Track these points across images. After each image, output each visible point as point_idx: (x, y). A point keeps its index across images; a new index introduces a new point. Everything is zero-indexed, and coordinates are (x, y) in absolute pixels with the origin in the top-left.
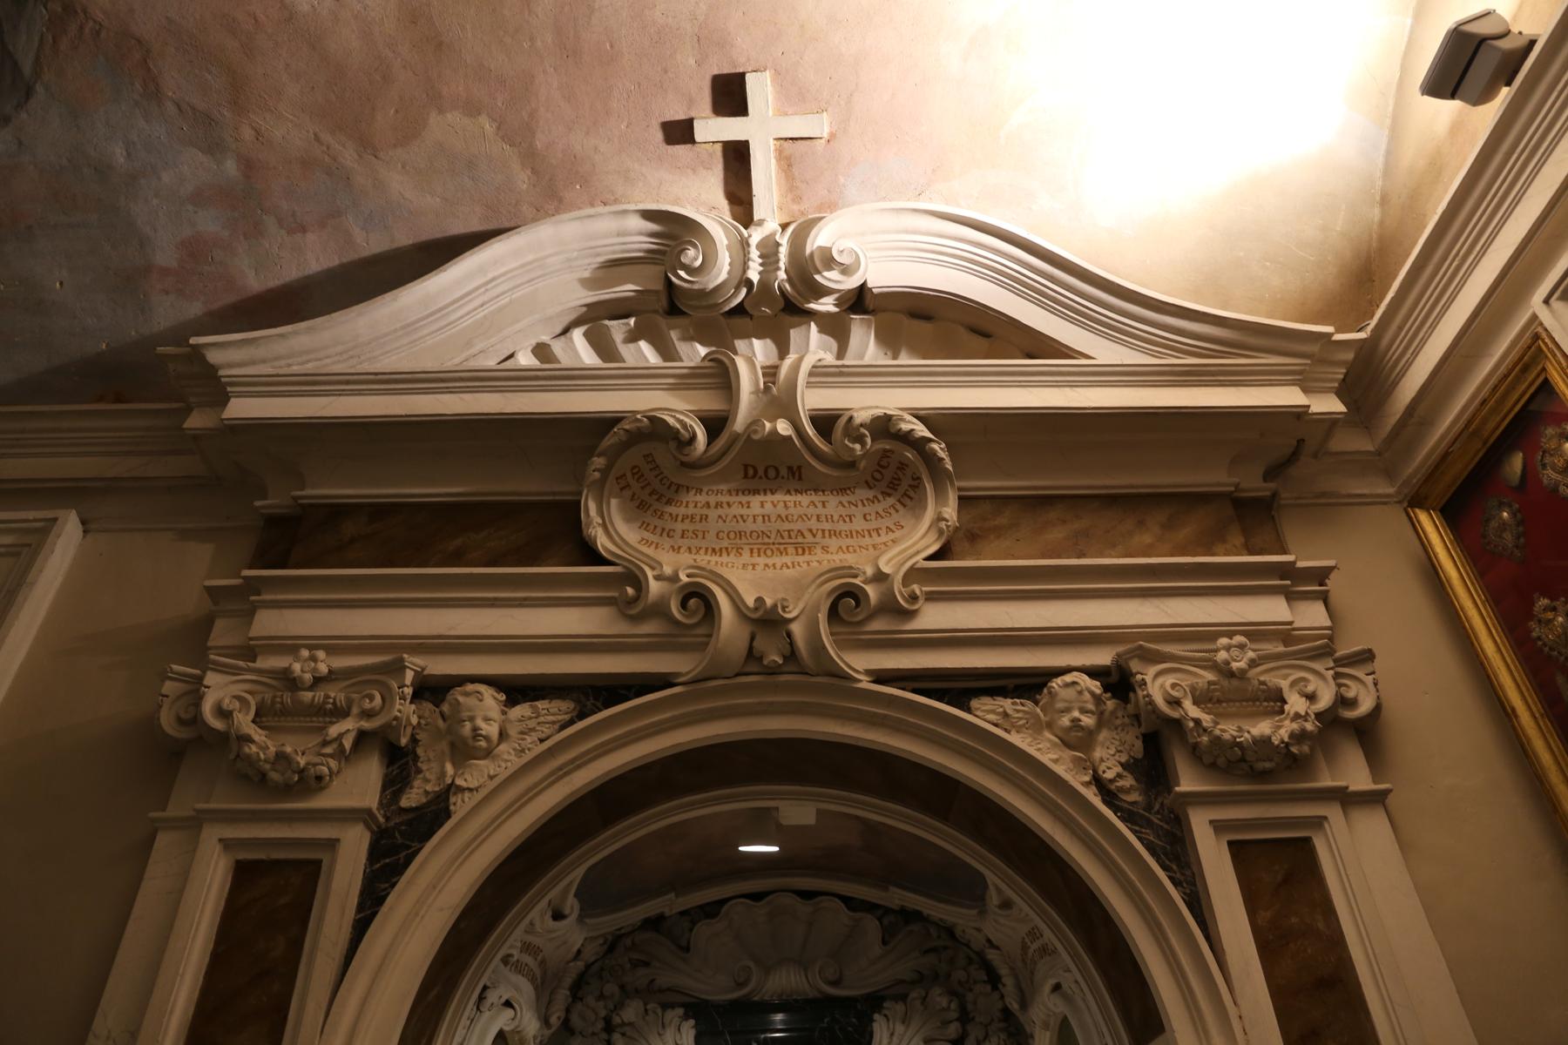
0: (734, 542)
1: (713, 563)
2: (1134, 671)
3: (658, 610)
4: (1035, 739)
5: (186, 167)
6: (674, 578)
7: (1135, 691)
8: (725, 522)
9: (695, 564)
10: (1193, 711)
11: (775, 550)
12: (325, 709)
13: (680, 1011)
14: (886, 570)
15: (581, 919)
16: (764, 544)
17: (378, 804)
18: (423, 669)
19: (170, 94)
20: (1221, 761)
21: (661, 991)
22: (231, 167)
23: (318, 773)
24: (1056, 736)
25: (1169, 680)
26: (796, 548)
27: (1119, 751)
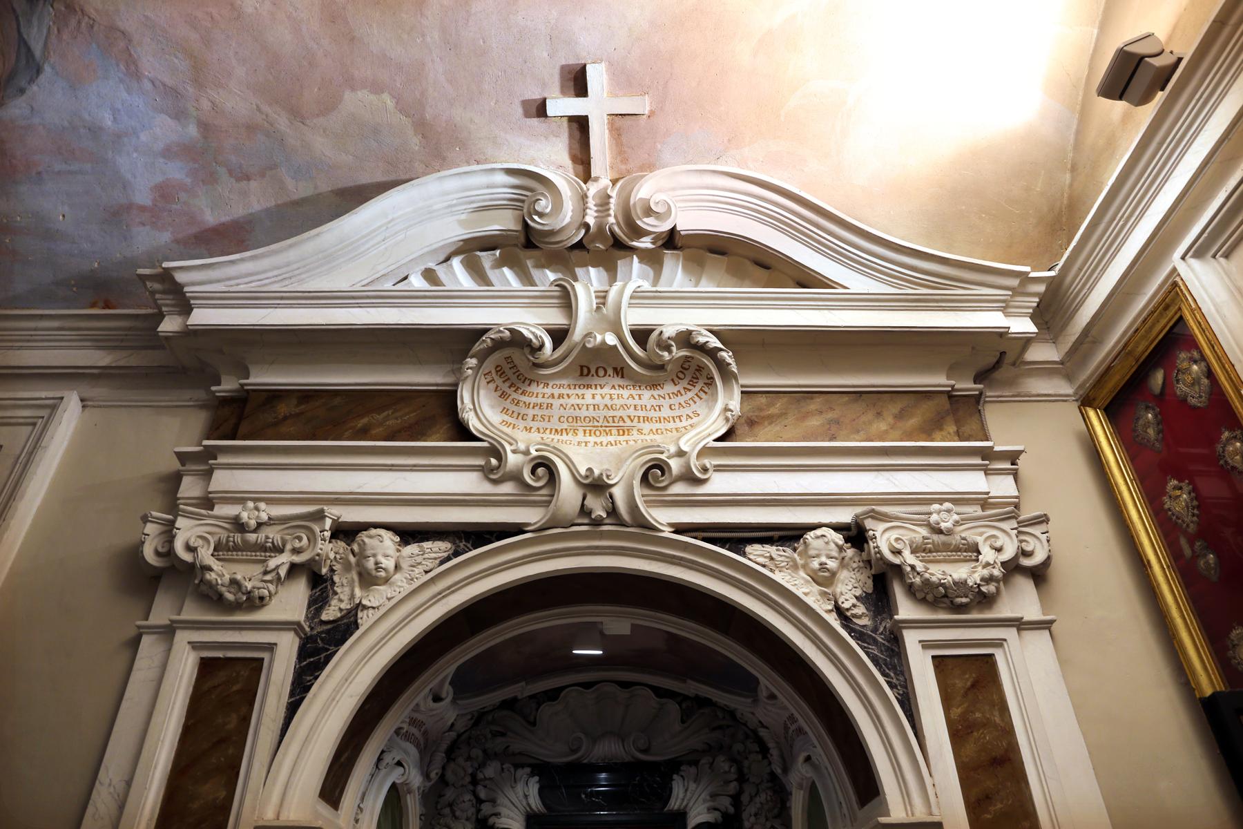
0: (572, 424)
1: (555, 440)
2: (868, 528)
3: (516, 477)
4: (793, 577)
5: (158, 129)
6: (527, 453)
7: (868, 543)
8: (565, 409)
9: (542, 441)
10: (909, 558)
11: (602, 432)
12: (266, 547)
13: (528, 770)
14: (685, 448)
15: (454, 701)
16: (594, 427)
17: (305, 617)
18: (339, 518)
19: (147, 73)
20: (930, 597)
21: (514, 754)
22: (193, 130)
23: (261, 595)
24: (810, 576)
25: (894, 535)
26: (618, 430)
27: (855, 587)
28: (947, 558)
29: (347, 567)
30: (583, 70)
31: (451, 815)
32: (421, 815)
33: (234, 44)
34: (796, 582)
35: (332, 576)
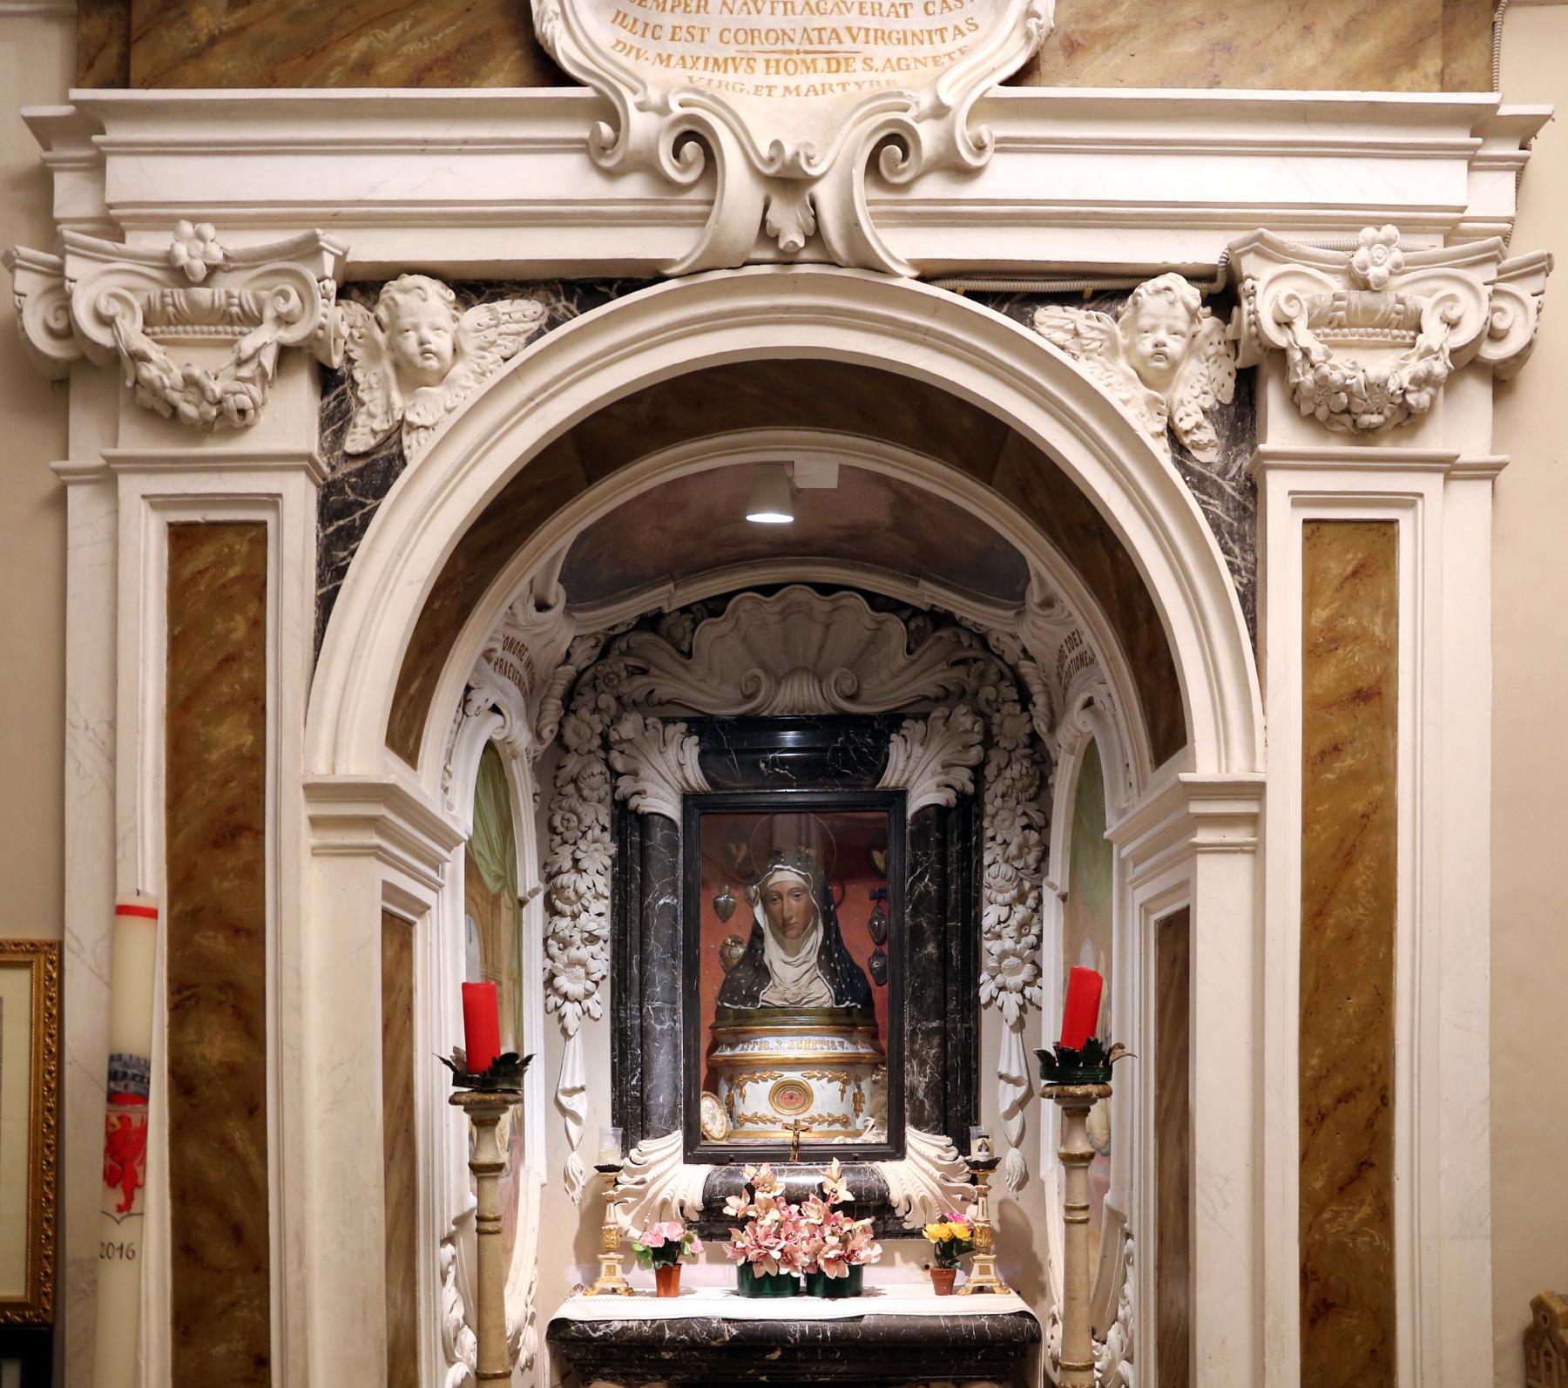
0: (743, 47)
1: (715, 84)
2: (1245, 273)
3: (646, 164)
4: (1107, 370)
6: (663, 110)
7: (1239, 305)
8: (731, 12)
9: (690, 85)
10: (1303, 336)
11: (799, 63)
12: (231, 315)
13: (682, 726)
14: (947, 100)
15: (568, 611)
16: (785, 52)
17: (319, 449)
18: (346, 253)
20: (1322, 413)
23: (240, 406)
24: (1133, 368)
26: (828, 60)
27: (1205, 393)
28: (1365, 338)
29: (374, 353)
31: (577, 795)
32: (535, 794)
34: (1110, 380)
35: (350, 371)
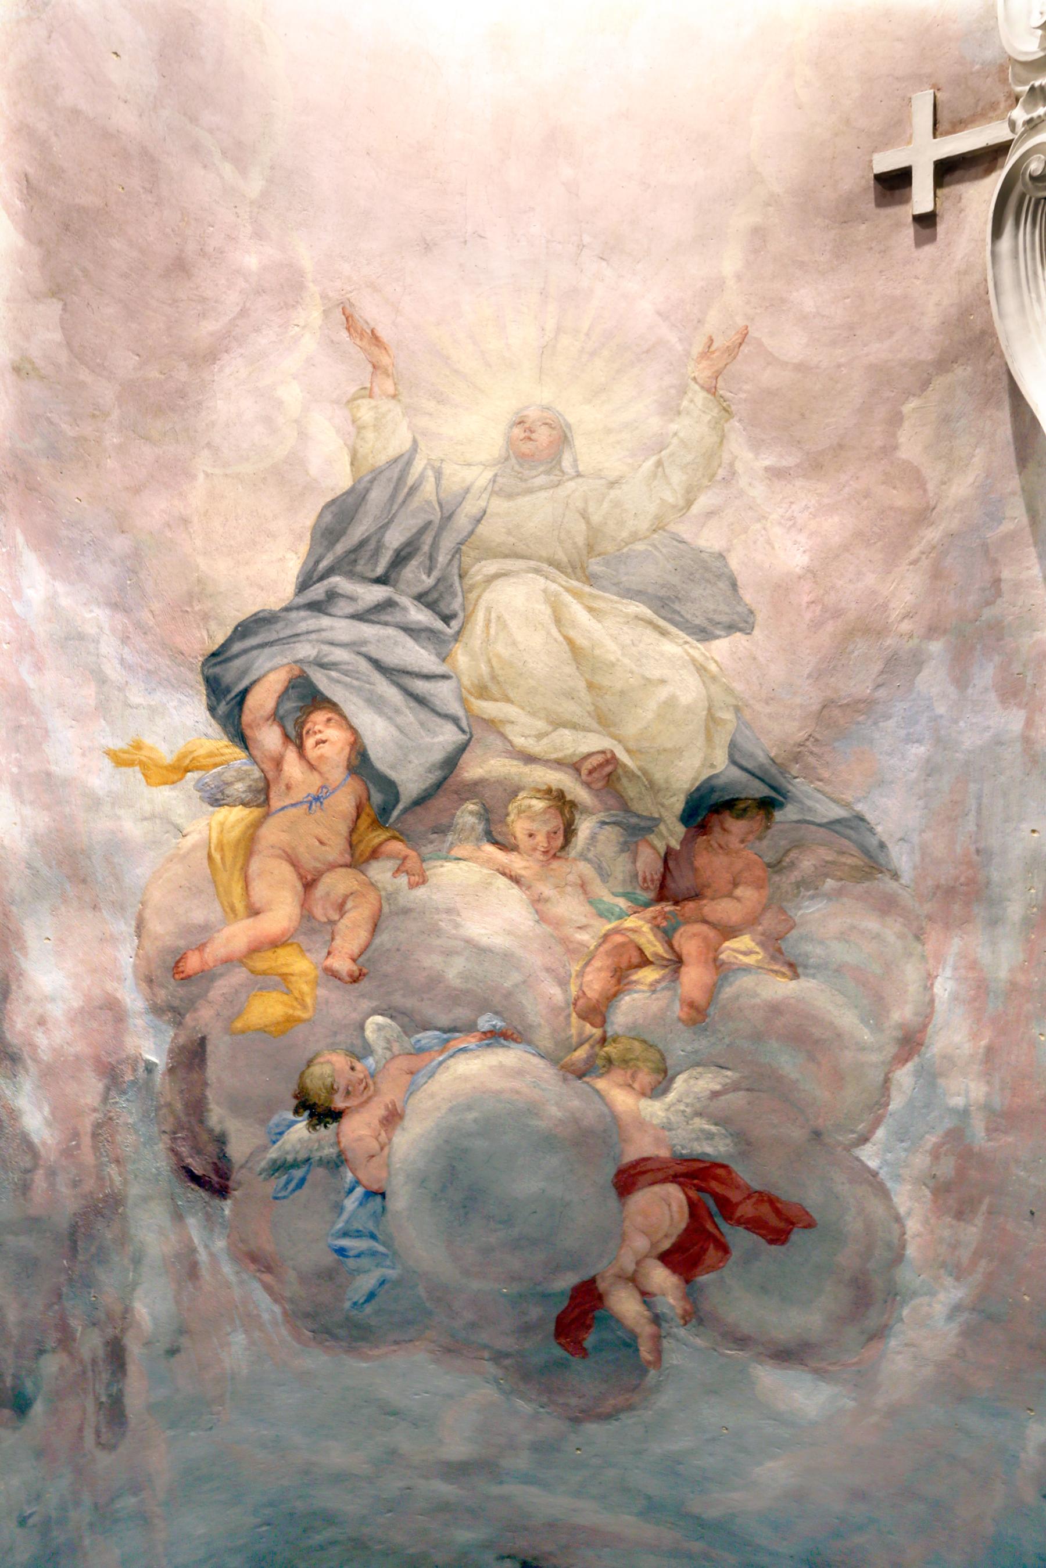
19: (869, 691)
22: (936, 647)
30: (881, 178)
33: (841, 582)
